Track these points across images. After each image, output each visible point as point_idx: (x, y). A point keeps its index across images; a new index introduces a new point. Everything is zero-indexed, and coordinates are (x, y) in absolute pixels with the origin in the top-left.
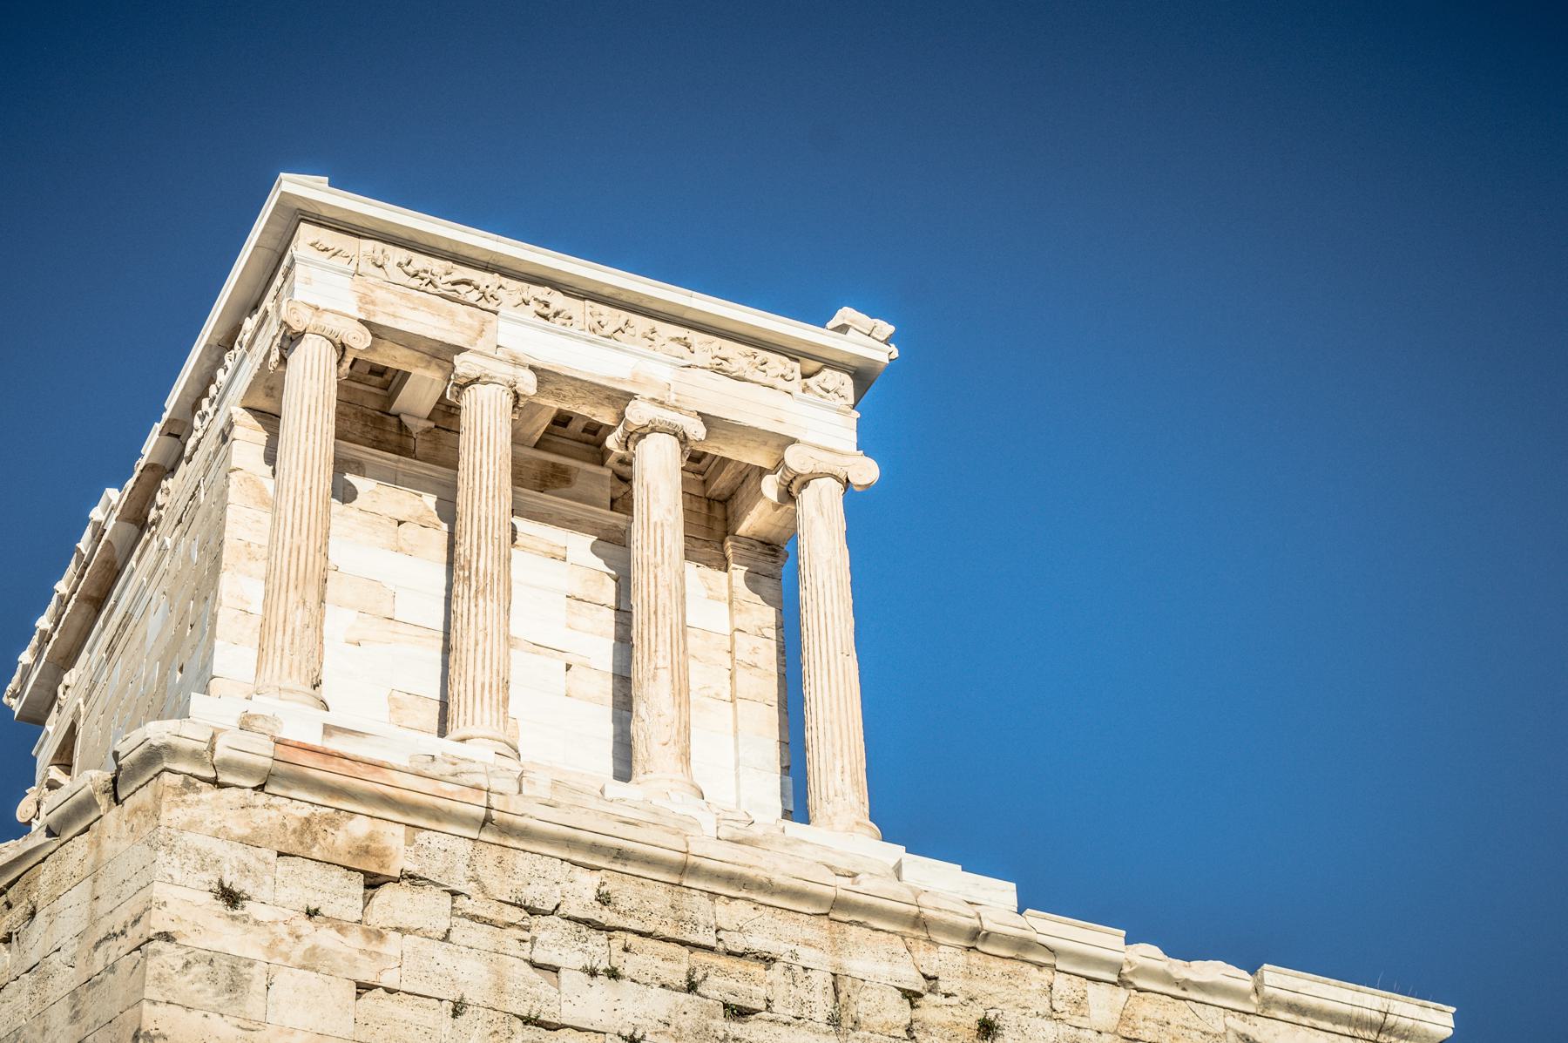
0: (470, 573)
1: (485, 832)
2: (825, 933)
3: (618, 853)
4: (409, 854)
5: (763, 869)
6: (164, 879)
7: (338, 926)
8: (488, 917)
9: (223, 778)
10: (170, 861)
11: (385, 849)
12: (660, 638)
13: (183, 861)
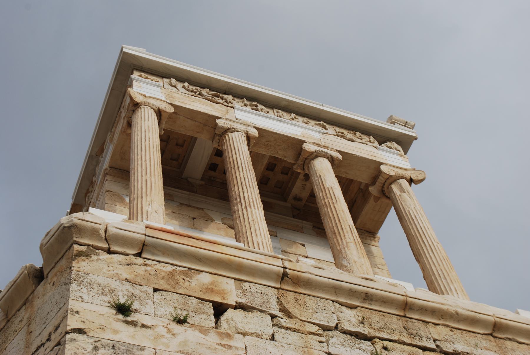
0: (240, 199)
1: (284, 283)
2: (494, 344)
3: (366, 296)
4: (239, 294)
5: (451, 306)
6: (75, 299)
7: (200, 329)
8: (296, 328)
9: (114, 248)
10: (80, 289)
11: (223, 290)
12: (345, 231)
13: (89, 289)
